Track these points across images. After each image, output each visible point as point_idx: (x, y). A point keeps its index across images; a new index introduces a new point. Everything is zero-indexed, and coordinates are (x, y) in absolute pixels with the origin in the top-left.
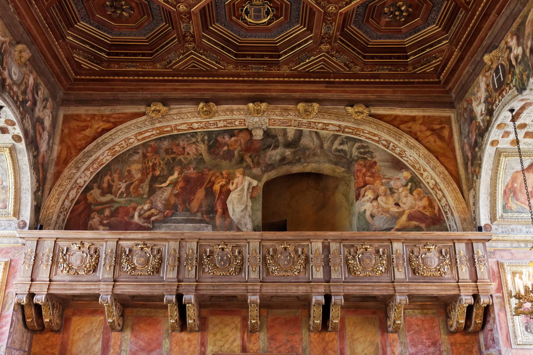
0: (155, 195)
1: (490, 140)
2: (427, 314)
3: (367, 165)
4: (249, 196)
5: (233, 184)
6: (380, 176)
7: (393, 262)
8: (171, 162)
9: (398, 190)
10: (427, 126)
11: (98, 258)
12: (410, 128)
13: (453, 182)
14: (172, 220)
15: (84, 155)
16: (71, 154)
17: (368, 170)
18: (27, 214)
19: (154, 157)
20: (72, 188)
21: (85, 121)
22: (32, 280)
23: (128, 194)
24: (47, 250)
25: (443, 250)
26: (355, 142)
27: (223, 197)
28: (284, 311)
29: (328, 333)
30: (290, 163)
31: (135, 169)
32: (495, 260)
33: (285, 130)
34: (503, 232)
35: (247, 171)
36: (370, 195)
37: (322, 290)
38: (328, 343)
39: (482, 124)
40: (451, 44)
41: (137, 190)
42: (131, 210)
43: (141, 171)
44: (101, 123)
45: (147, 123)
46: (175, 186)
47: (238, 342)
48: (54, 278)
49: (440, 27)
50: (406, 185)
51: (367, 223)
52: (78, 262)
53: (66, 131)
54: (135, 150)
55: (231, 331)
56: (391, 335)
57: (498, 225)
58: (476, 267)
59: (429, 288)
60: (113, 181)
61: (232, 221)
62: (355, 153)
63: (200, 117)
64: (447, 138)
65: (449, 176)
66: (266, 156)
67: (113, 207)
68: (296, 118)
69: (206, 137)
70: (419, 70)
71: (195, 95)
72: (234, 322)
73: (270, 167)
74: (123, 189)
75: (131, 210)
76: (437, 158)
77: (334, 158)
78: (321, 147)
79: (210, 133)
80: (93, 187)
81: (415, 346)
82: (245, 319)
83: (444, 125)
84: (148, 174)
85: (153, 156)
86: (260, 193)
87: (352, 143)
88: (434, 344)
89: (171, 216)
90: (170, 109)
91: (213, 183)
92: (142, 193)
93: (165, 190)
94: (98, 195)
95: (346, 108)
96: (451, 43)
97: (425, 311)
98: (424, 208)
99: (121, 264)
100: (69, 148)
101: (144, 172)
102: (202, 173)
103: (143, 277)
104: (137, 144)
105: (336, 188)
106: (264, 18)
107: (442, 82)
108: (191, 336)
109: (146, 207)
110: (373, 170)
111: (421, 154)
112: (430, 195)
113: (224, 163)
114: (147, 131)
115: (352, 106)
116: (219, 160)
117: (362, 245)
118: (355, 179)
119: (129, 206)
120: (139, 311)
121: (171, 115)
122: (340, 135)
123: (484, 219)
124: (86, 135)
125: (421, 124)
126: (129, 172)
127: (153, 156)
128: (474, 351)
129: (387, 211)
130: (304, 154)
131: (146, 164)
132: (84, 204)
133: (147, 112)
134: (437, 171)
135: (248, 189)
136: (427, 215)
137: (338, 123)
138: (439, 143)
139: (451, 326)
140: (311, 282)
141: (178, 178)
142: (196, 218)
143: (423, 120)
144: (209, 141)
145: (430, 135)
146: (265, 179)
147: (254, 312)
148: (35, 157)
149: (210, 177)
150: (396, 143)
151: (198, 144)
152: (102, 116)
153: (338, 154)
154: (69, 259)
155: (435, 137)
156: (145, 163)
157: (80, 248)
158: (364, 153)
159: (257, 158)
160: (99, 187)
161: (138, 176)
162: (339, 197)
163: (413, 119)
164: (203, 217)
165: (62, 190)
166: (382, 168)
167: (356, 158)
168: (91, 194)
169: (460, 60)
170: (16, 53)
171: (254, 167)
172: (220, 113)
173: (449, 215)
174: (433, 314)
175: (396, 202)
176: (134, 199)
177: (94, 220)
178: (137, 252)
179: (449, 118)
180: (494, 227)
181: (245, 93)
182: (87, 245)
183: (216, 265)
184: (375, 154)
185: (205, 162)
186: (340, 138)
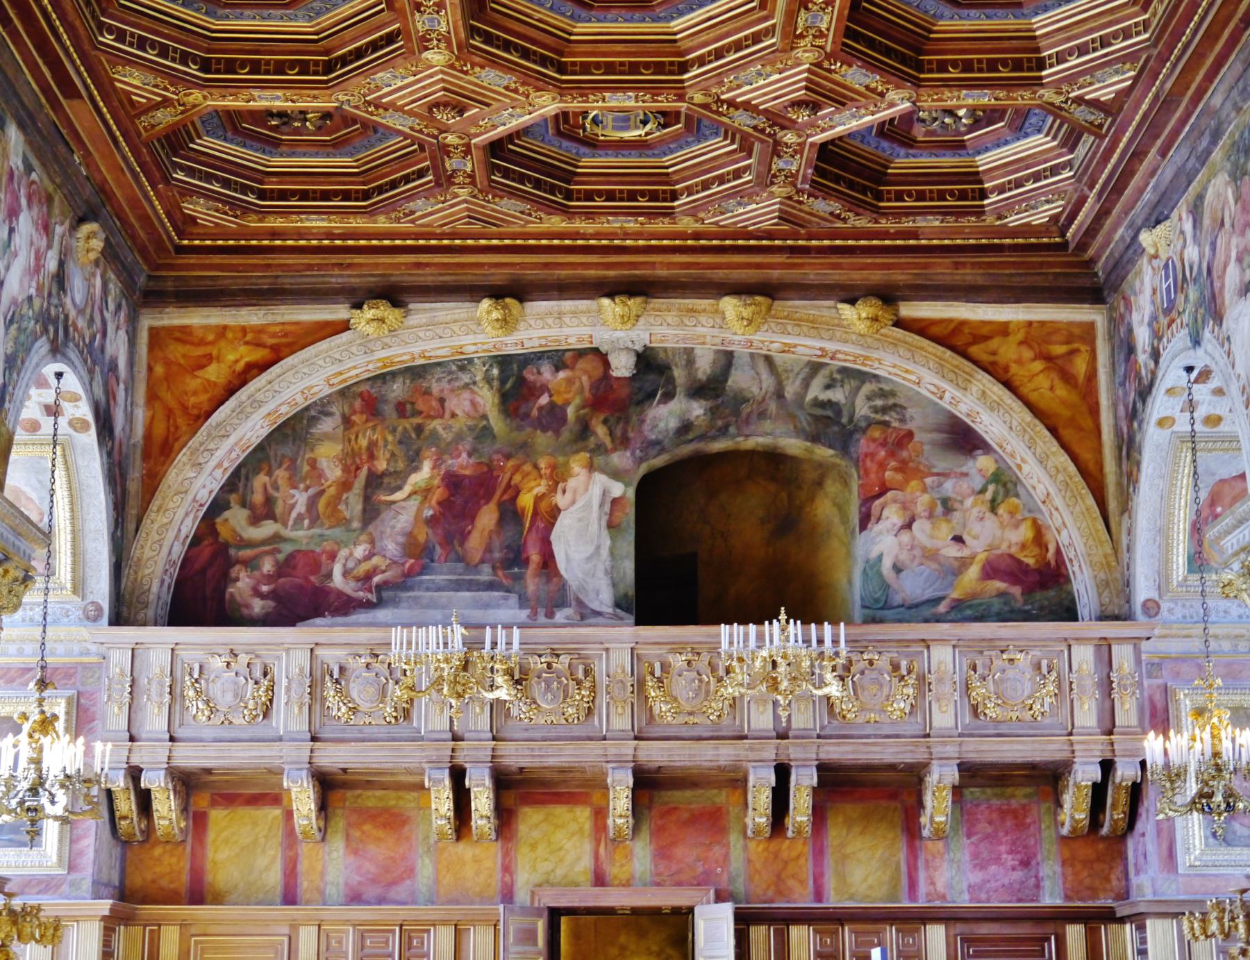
0: (378, 522)
1: (1153, 420)
2: (1013, 796)
3: (890, 440)
4: (604, 523)
5: (564, 492)
6: (921, 467)
7: (930, 690)
8: (413, 436)
9: (962, 502)
10: (1036, 346)
11: (271, 688)
12: (994, 353)
13: (1086, 491)
14: (421, 582)
15: (209, 435)
16: (177, 428)
17: (892, 454)
18: (100, 588)
19: (371, 424)
20: (187, 514)
21: (202, 342)
22: (132, 739)
24: (158, 671)
25: (1044, 663)
26: (863, 382)
28: (688, 794)
29: (787, 842)
30: (702, 437)
32: (1160, 681)
33: (689, 352)
34: (1184, 617)
35: (599, 460)
36: (892, 516)
37: (769, 752)
38: (786, 863)
39: (1143, 372)
40: (1079, 181)
41: (335, 510)
42: (324, 558)
43: (341, 461)
44: (243, 349)
45: (354, 349)
46: (426, 498)
47: (586, 863)
48: (179, 733)
49: (1054, 138)
50: (983, 491)
51: (886, 587)
52: (229, 697)
53: (159, 370)
54: (323, 405)
55: (569, 839)
56: (929, 844)
57: (1174, 601)
58: (1113, 700)
59: (1006, 747)
60: (277, 489)
61: (563, 586)
62: (862, 409)
63: (483, 332)
64: (1081, 378)
65: (1078, 478)
66: (643, 421)
67: (280, 552)
68: (716, 331)
69: (495, 371)
70: (1013, 220)
71: (468, 278)
72: (575, 820)
73: (656, 445)
74: (301, 507)
75: (324, 558)
76: (1053, 431)
77: (809, 424)
78: (779, 395)
79: (504, 361)
80: (229, 503)
81: (982, 866)
82: (600, 814)
83: (1076, 345)
84: (358, 468)
85: (367, 421)
86: (629, 515)
87: (854, 383)
88: (1025, 863)
89: (421, 574)
90: (407, 314)
91: (518, 492)
92: (347, 514)
93: (403, 508)
94: (243, 523)
95: (840, 306)
96: (1078, 178)
97: (1009, 790)
98: (1023, 546)
99: (324, 699)
100: (169, 413)
101: (350, 465)
102: (490, 468)
103: (375, 729)
104: (327, 391)
105: (819, 483)
106: (637, 128)
107: (1072, 246)
108: (478, 851)
109: (359, 551)
110: (905, 454)
111: (1015, 423)
112: (1038, 516)
113: (543, 439)
114: (355, 367)
115: (852, 302)
116: (529, 430)
117: (862, 653)
118: (859, 477)
119: (318, 550)
120: (359, 796)
121: (412, 327)
122: (827, 364)
123: (1143, 590)
124: (208, 381)
125: (1021, 343)
126: (313, 463)
127: (367, 421)
128: (1113, 877)
129: (931, 555)
130: (737, 413)
131: (353, 442)
132: (211, 545)
133: (352, 321)
134: (1050, 464)
135: (601, 505)
136: (1027, 565)
137: (818, 344)
138: (1062, 391)
139: (1063, 824)
140: (745, 737)
141: (432, 478)
142: (479, 577)
143: (1028, 333)
144: (503, 381)
145: (1042, 371)
146: (643, 469)
147: (620, 801)
148: (110, 454)
149: (508, 475)
150: (958, 394)
151: (475, 389)
152: (244, 330)
153: (819, 412)
154: (207, 689)
155: (1054, 375)
156: (349, 441)
157: (229, 664)
158: (884, 410)
159: (621, 425)
160: (244, 504)
161: (334, 473)
162: (824, 509)
163: (1003, 329)
164: (495, 574)
165: (165, 521)
166: (926, 448)
167: (863, 424)
168: (226, 520)
169: (1103, 214)
170: (82, 243)
171: (615, 449)
172: (532, 322)
173: (1076, 568)
174: (1026, 796)
175: (958, 533)
176: (328, 532)
177: (239, 584)
178: (357, 673)
179: (1091, 326)
180: (1165, 606)
181: (592, 273)
182: (243, 659)
183: (535, 702)
184: (910, 412)
185: (494, 437)
186: (824, 372)
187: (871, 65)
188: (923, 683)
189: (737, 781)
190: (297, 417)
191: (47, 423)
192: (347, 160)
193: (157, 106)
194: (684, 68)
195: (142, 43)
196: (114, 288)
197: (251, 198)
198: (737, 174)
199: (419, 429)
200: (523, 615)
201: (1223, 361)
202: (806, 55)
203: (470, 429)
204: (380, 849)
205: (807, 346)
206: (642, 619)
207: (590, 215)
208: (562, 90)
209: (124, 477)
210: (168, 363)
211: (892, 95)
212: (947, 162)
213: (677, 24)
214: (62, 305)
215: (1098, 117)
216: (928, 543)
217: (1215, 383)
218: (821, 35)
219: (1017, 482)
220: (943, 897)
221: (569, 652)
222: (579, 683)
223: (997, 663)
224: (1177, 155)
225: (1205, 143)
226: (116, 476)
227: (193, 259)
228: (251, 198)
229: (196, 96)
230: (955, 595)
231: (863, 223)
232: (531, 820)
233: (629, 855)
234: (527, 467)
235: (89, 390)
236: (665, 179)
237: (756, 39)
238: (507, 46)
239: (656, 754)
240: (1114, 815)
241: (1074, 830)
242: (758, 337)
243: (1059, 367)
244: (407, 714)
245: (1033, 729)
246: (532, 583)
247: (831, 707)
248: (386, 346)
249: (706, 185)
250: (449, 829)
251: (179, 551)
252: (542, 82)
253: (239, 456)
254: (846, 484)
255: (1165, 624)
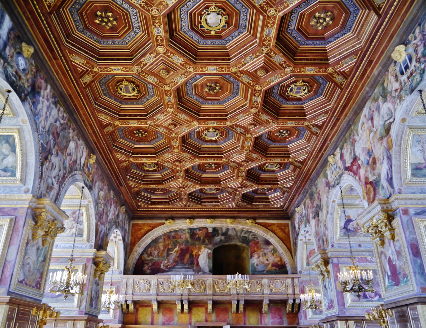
11: (150, 286)
13: (288, 252)
17: (256, 245)
21: (141, 226)
23: (159, 256)
27: (197, 257)
28: (222, 305)
30: (224, 242)
31: (161, 246)
33: (221, 228)
35: (207, 246)
36: (256, 256)
37: (236, 298)
44: (147, 227)
47: (204, 318)
48: (134, 294)
50: (271, 252)
51: (255, 268)
52: (143, 287)
56: (264, 315)
60: (152, 251)
61: (200, 268)
62: (251, 238)
65: (287, 250)
70: (275, 206)
73: (216, 244)
74: (156, 254)
76: (283, 241)
78: (237, 235)
82: (207, 309)
86: (211, 256)
88: (281, 318)
90: (175, 221)
91: (193, 252)
96: (285, 199)
98: (278, 261)
100: (135, 238)
101: (165, 246)
105: (244, 250)
109: (166, 262)
113: (197, 243)
115: (248, 220)
123: (299, 269)
125: (277, 226)
126: (158, 247)
129: (263, 263)
130: (229, 238)
138: (284, 235)
144: (190, 232)
146: (214, 248)
147: (210, 306)
152: (148, 224)
160: (147, 253)
161: (162, 248)
162: (244, 255)
163: (274, 224)
169: (289, 205)
180: (303, 272)
184: (259, 238)
187: (251, 181)
188: (262, 285)
189: (230, 303)
190: (156, 239)
191: (114, 240)
192: (165, 196)
193: (135, 187)
194: (220, 181)
195: (133, 178)
196: (127, 217)
197: (150, 202)
198: (229, 199)
199: (176, 241)
200: (193, 273)
201: (310, 230)
202: (240, 180)
203: (185, 241)
204: (168, 315)
205: (241, 227)
206: (214, 274)
207: (205, 205)
208: (201, 185)
209: (127, 248)
210: (135, 230)
211: (254, 186)
212: (264, 197)
213: (219, 175)
214: (118, 220)
215: (288, 190)
216: (262, 261)
217: (309, 233)
218: (242, 176)
219: (277, 250)
220: (267, 324)
221: (201, 280)
222: (203, 285)
223: (275, 282)
224: (301, 196)
225: (305, 194)
226: (125, 249)
227: (139, 212)
228: (150, 202)
229: (141, 186)
230: (267, 270)
231: (250, 207)
232: (195, 310)
233: (212, 316)
234: (194, 247)
235: (122, 234)
236: (217, 199)
237: (232, 177)
238: (192, 178)
239: (216, 298)
240: (296, 309)
241: (289, 312)
242: (233, 225)
243: (283, 230)
244: (173, 291)
245: (281, 294)
246: (195, 268)
247: (246, 290)
248: (171, 227)
249: (224, 200)
250: (180, 312)
251: (135, 261)
252: (197, 184)
253: (146, 245)
254: (248, 250)
255: (303, 275)
